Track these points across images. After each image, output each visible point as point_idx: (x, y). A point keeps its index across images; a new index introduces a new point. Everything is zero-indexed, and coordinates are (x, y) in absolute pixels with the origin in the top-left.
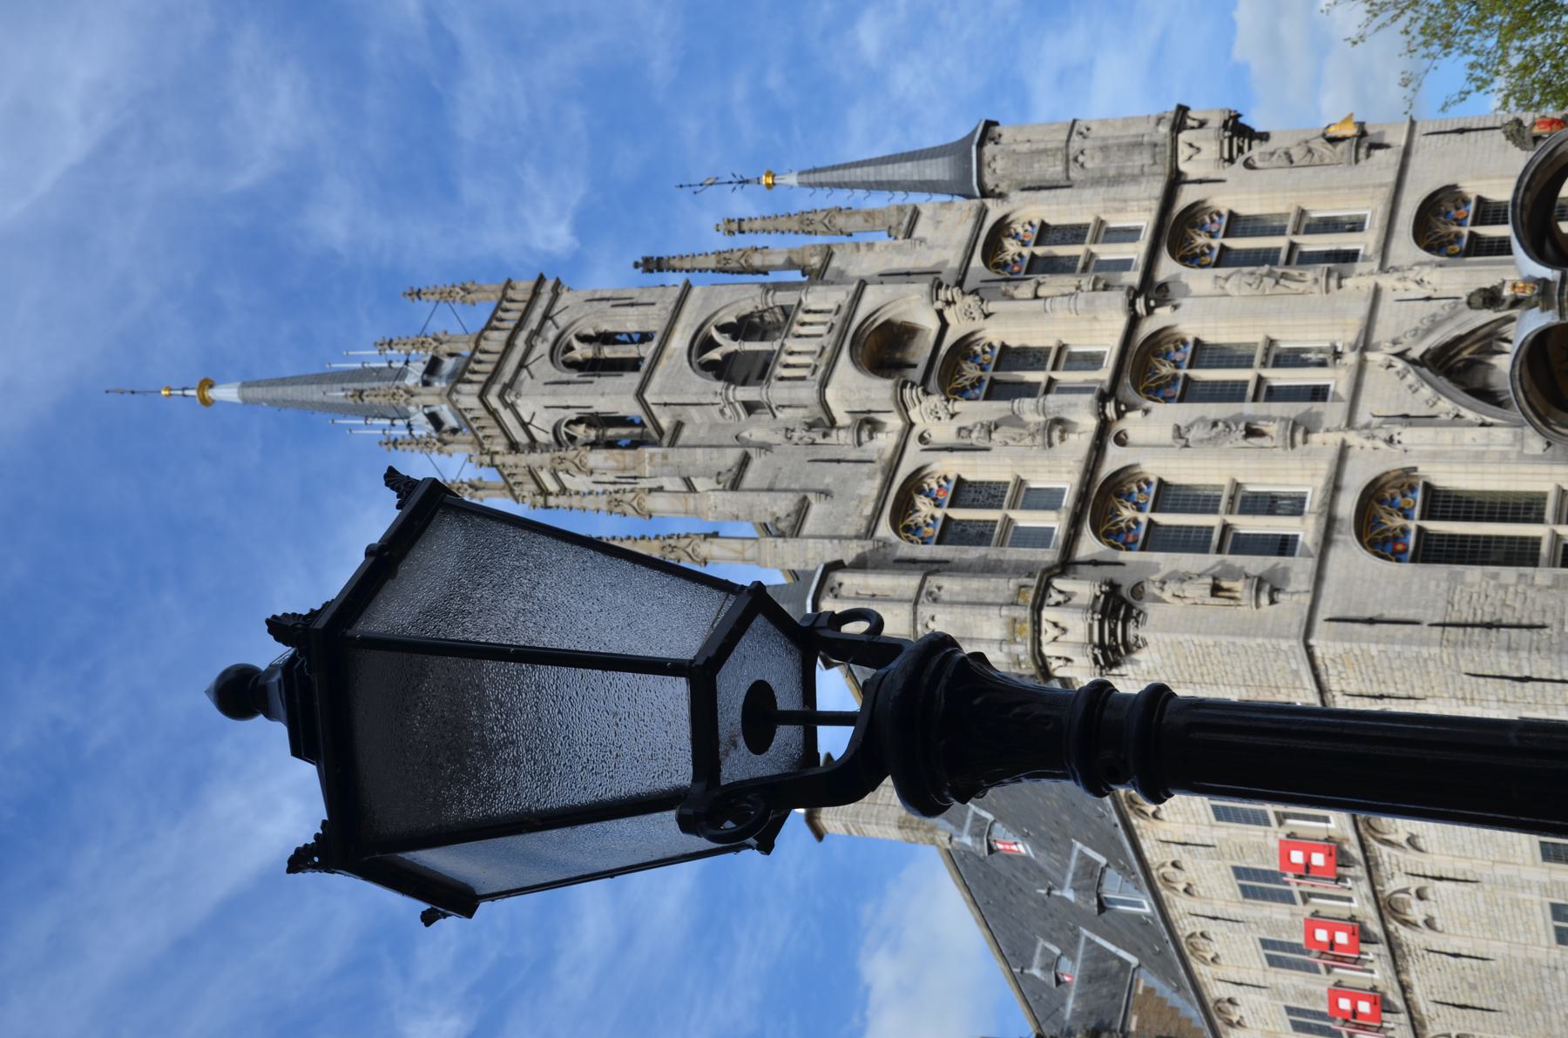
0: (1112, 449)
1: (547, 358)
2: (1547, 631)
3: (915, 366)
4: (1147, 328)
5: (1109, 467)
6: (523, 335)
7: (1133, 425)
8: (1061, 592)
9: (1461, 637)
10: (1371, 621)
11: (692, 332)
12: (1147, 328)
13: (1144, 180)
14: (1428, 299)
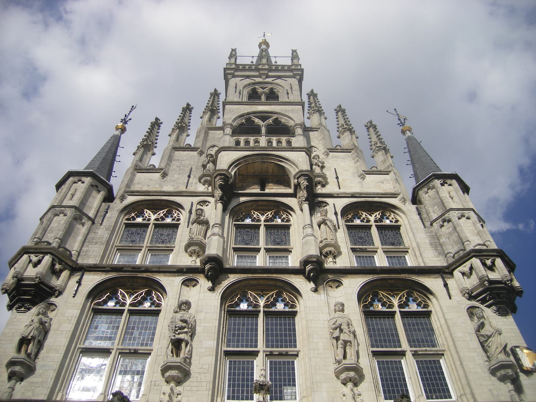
5: (163, 279)
8: (39, 262)
13: (441, 258)
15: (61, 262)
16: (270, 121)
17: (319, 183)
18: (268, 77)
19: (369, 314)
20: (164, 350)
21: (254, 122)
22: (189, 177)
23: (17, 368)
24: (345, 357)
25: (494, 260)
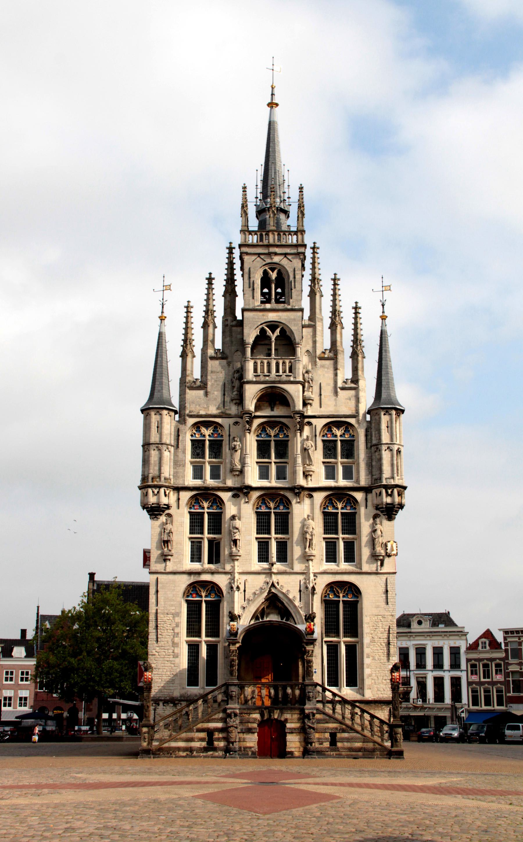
0: (230, 494)
1: (264, 263)
3: (272, 410)
4: (289, 495)
5: (221, 494)
10: (157, 591)
12: (289, 495)
13: (370, 476)
14: (300, 591)
16: (277, 332)
17: (308, 404)
18: (276, 254)
19: (326, 514)
22: (224, 395)
25: (393, 490)
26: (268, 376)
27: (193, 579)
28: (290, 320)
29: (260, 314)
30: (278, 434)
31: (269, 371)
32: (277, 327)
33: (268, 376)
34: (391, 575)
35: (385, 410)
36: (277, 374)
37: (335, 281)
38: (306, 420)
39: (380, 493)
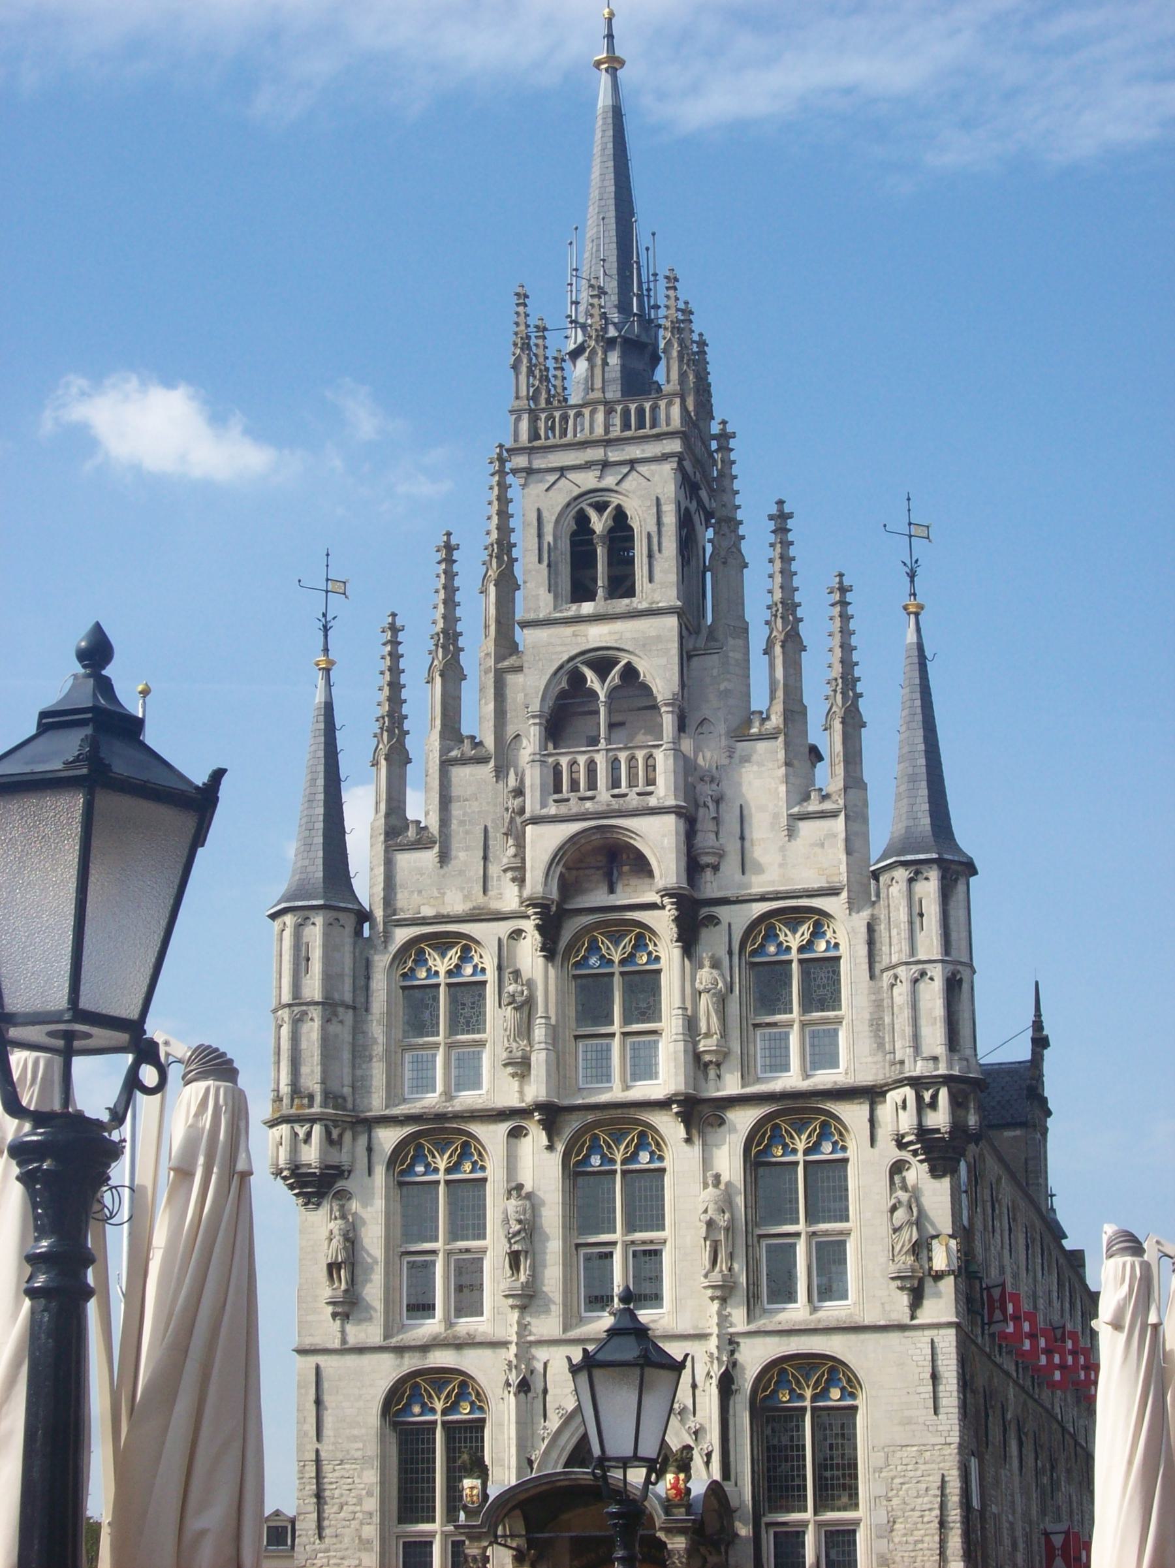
0: (504, 1128)
1: (577, 491)
2: (318, 1541)
3: (612, 890)
5: (480, 1130)
6: (597, 454)
7: (536, 1136)
8: (309, 1135)
9: (307, 1475)
10: (318, 1402)
11: (604, 644)
13: (879, 1057)
15: (336, 1123)
16: (614, 674)
17: (708, 866)
18: (605, 465)
20: (501, 1259)
21: (584, 679)
23: (339, 1310)
24: (714, 1262)
26: (592, 798)
27: (411, 1363)
28: (646, 644)
29: (568, 631)
30: (632, 956)
31: (592, 785)
32: (612, 663)
33: (592, 798)
34: (942, 1332)
35: (913, 868)
36: (616, 791)
37: (781, 520)
38: (705, 911)
39: (904, 1101)
